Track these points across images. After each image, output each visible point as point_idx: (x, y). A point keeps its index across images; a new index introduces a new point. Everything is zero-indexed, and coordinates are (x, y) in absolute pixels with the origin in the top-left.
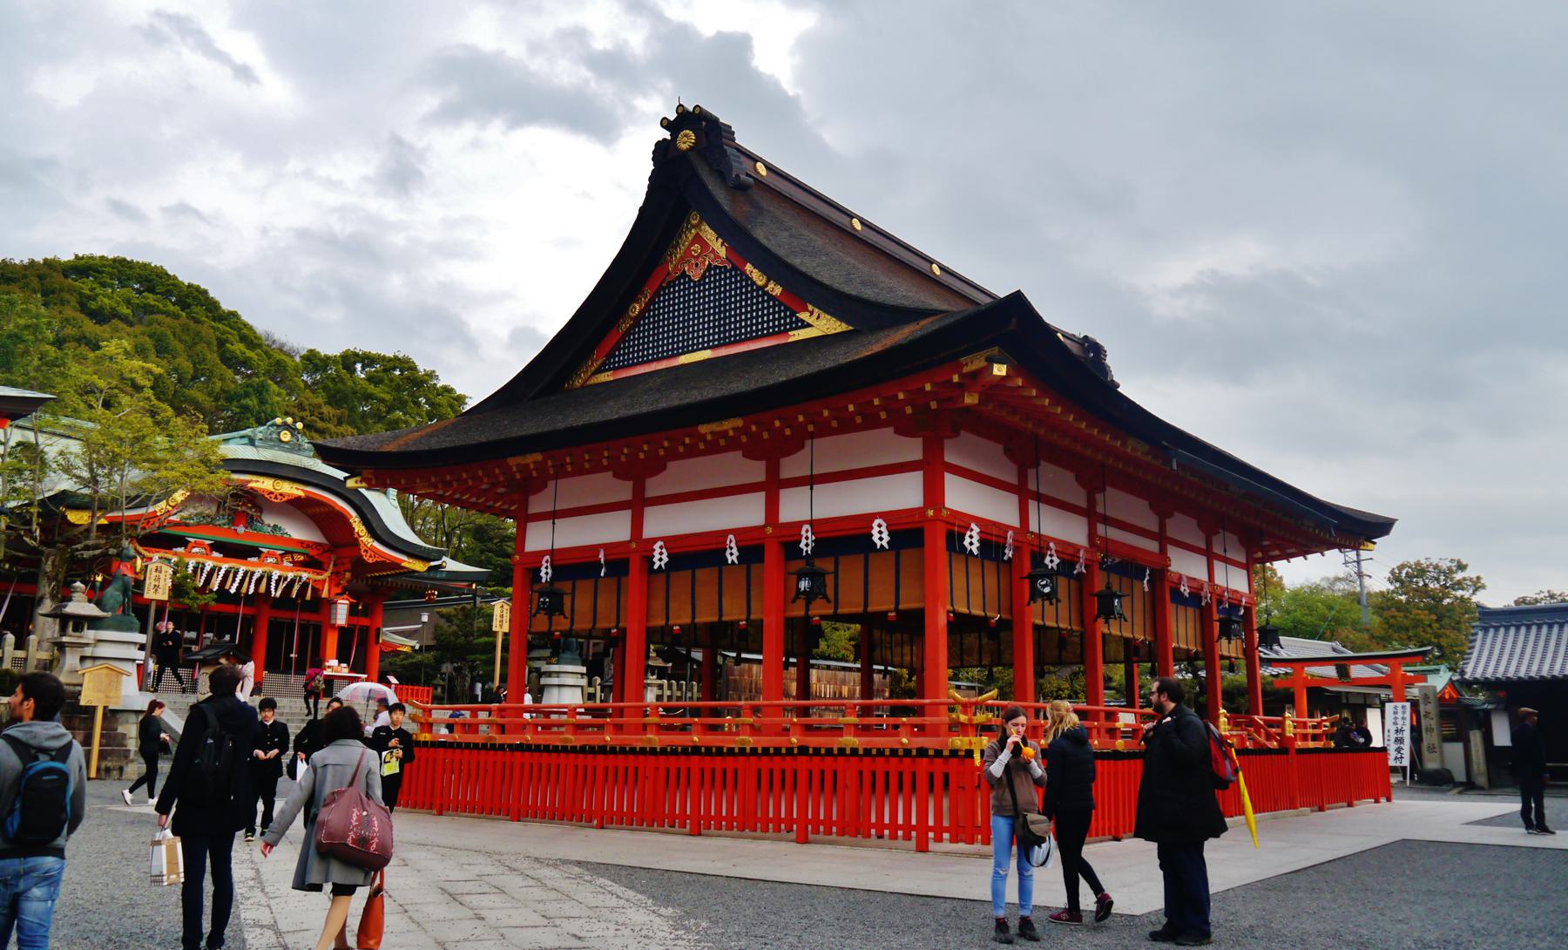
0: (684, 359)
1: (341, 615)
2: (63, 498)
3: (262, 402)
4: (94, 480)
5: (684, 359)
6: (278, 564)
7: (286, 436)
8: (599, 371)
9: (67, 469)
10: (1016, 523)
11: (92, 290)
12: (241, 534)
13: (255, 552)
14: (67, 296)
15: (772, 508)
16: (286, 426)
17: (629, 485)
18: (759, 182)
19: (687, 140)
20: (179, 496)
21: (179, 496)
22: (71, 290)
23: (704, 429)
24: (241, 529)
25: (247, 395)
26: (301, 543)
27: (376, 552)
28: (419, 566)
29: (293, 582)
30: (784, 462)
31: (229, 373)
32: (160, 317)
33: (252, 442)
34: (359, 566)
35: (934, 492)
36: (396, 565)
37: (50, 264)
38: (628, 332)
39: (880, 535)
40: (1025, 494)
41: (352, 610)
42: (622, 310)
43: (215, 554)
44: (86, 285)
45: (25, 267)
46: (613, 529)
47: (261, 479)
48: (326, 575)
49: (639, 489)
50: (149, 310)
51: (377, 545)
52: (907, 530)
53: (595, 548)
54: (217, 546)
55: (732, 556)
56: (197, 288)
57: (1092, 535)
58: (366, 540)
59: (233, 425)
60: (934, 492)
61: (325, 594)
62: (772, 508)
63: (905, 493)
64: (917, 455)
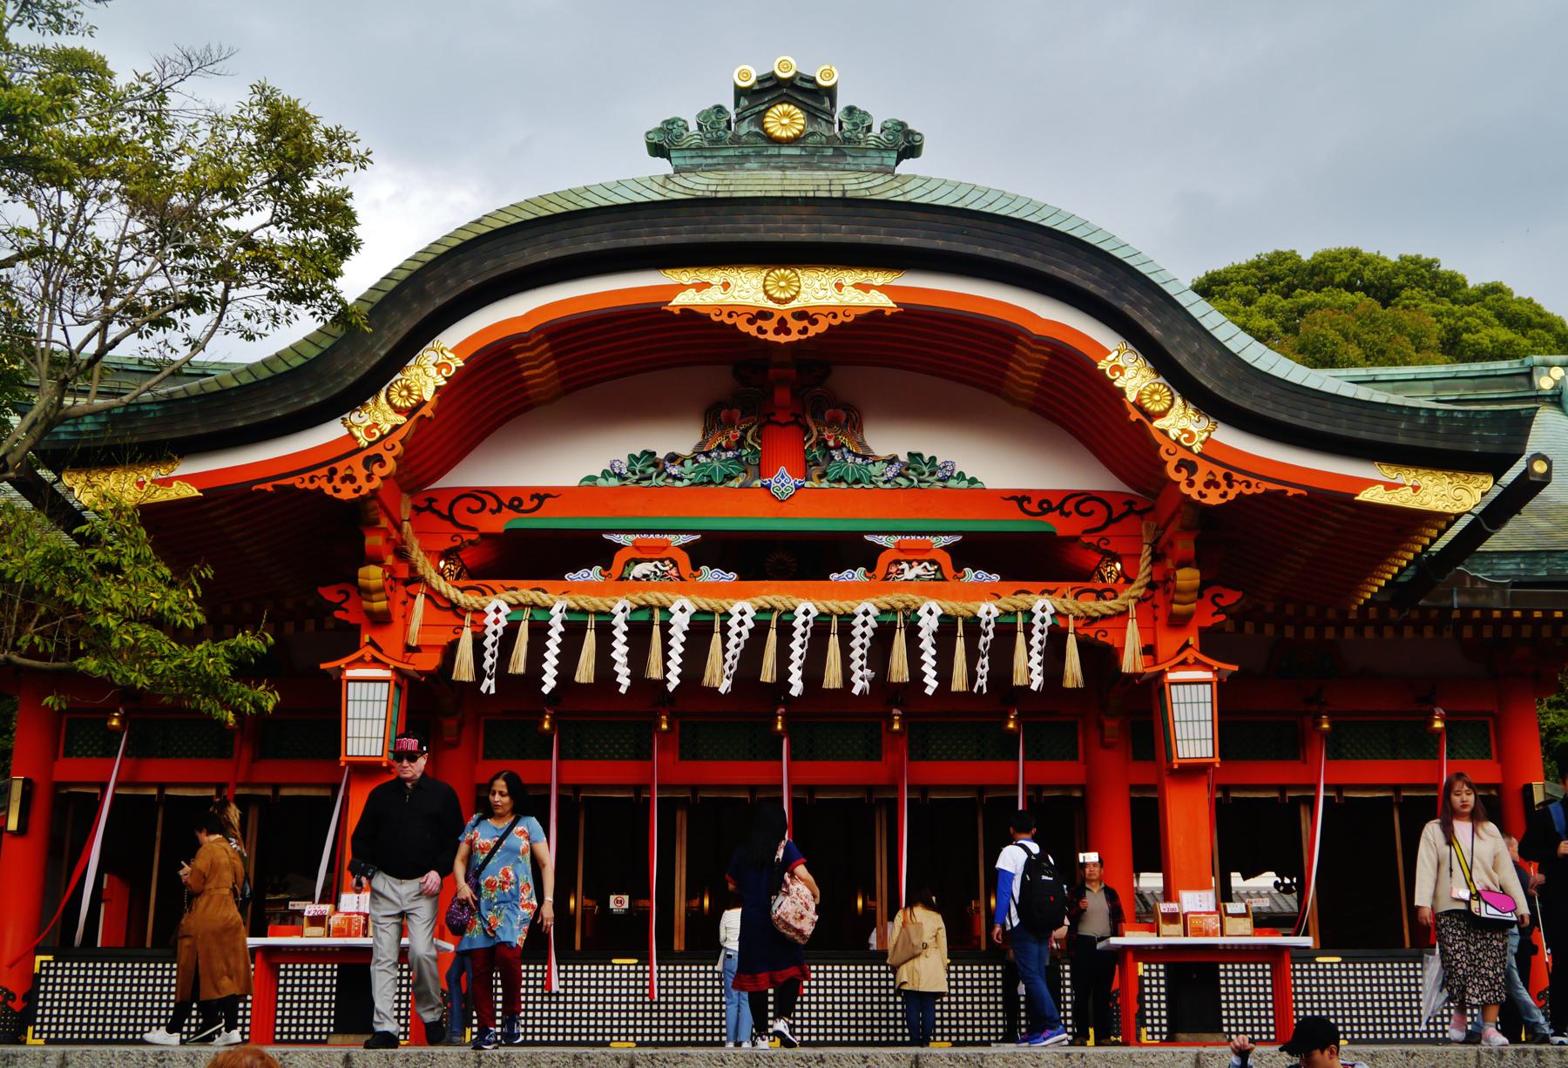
1: (1193, 727)
12: (785, 498)
24: (783, 481)
26: (1020, 499)
27: (1230, 467)
28: (1452, 495)
29: (1006, 633)
36: (1336, 504)
43: (709, 575)
47: (716, 276)
48: (1128, 597)
51: (1228, 437)
54: (716, 549)
56: (1416, 261)
58: (1180, 423)
61: (1131, 661)
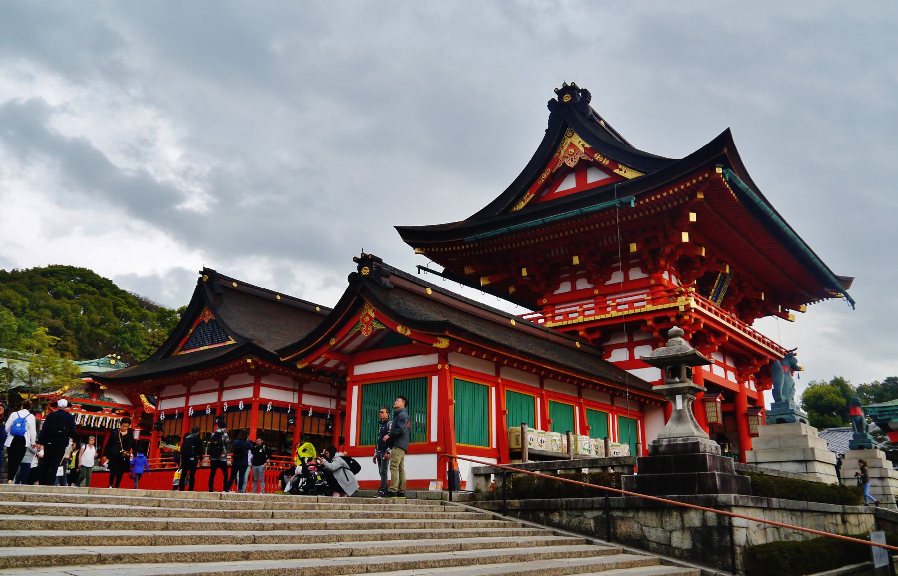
0: (202, 349)
2: (20, 389)
3: (133, 335)
4: (30, 382)
5: (202, 349)
6: (109, 414)
7: (113, 362)
8: (180, 351)
9: (21, 378)
10: (296, 401)
11: (55, 282)
13: (100, 409)
14: (42, 286)
15: (220, 397)
16: (113, 358)
17: (185, 389)
18: (233, 289)
19: (206, 278)
20: (66, 387)
21: (66, 387)
22: (44, 283)
23: (190, 373)
24: (94, 400)
25: (126, 332)
26: (121, 405)
30: (225, 382)
31: (117, 320)
32: (86, 295)
33: (98, 365)
34: (144, 414)
35: (257, 393)
37: (36, 270)
38: (189, 338)
39: (241, 406)
40: (301, 392)
41: (141, 434)
42: (187, 331)
44: (52, 281)
45: (23, 272)
46: (179, 403)
49: (188, 390)
50: (83, 291)
52: (248, 404)
53: (175, 409)
54: (84, 407)
55: (208, 411)
57: (338, 404)
59: (90, 356)
60: (257, 393)
62: (220, 397)
63: (248, 393)
64: (252, 381)
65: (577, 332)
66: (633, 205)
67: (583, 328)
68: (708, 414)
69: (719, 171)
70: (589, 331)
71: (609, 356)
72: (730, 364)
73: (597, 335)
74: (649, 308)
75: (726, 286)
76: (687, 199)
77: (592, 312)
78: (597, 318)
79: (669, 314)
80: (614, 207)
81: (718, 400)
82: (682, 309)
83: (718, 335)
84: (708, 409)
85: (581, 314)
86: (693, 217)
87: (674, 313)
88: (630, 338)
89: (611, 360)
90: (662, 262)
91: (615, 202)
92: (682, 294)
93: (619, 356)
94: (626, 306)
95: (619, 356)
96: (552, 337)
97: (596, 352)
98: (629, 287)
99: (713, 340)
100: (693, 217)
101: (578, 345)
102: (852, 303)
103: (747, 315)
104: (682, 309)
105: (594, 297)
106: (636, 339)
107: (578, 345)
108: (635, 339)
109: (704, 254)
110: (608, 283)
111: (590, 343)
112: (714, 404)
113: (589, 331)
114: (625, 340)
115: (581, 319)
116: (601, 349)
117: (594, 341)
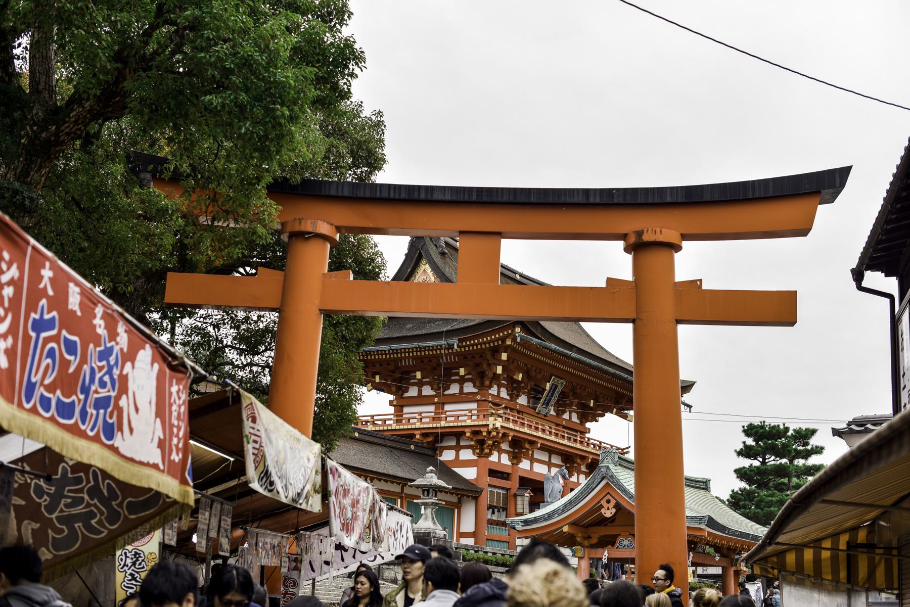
65: (415, 435)
66: (455, 347)
67: (419, 432)
68: (518, 506)
69: (518, 330)
70: (424, 435)
71: (441, 456)
72: (556, 460)
73: (430, 439)
74: (469, 422)
75: (557, 394)
76: (500, 342)
77: (428, 420)
78: (430, 426)
79: (482, 429)
80: (440, 348)
81: (527, 495)
82: (491, 427)
83: (532, 443)
84: (518, 502)
85: (420, 417)
86: (504, 356)
87: (486, 429)
88: (458, 442)
89: (442, 458)
90: (487, 383)
91: (442, 342)
92: (492, 414)
93: (448, 456)
94: (453, 419)
95: (448, 456)
96: (389, 443)
97: (430, 452)
98: (462, 398)
99: (527, 446)
100: (504, 356)
101: (412, 447)
102: (690, 407)
103: (589, 415)
104: (491, 427)
105: (435, 404)
106: (462, 443)
107: (412, 447)
108: (462, 443)
109: (520, 379)
110: (447, 392)
111: (425, 445)
112: (522, 498)
113: (424, 435)
114: (454, 443)
115: (418, 425)
116: (436, 449)
117: (428, 443)
